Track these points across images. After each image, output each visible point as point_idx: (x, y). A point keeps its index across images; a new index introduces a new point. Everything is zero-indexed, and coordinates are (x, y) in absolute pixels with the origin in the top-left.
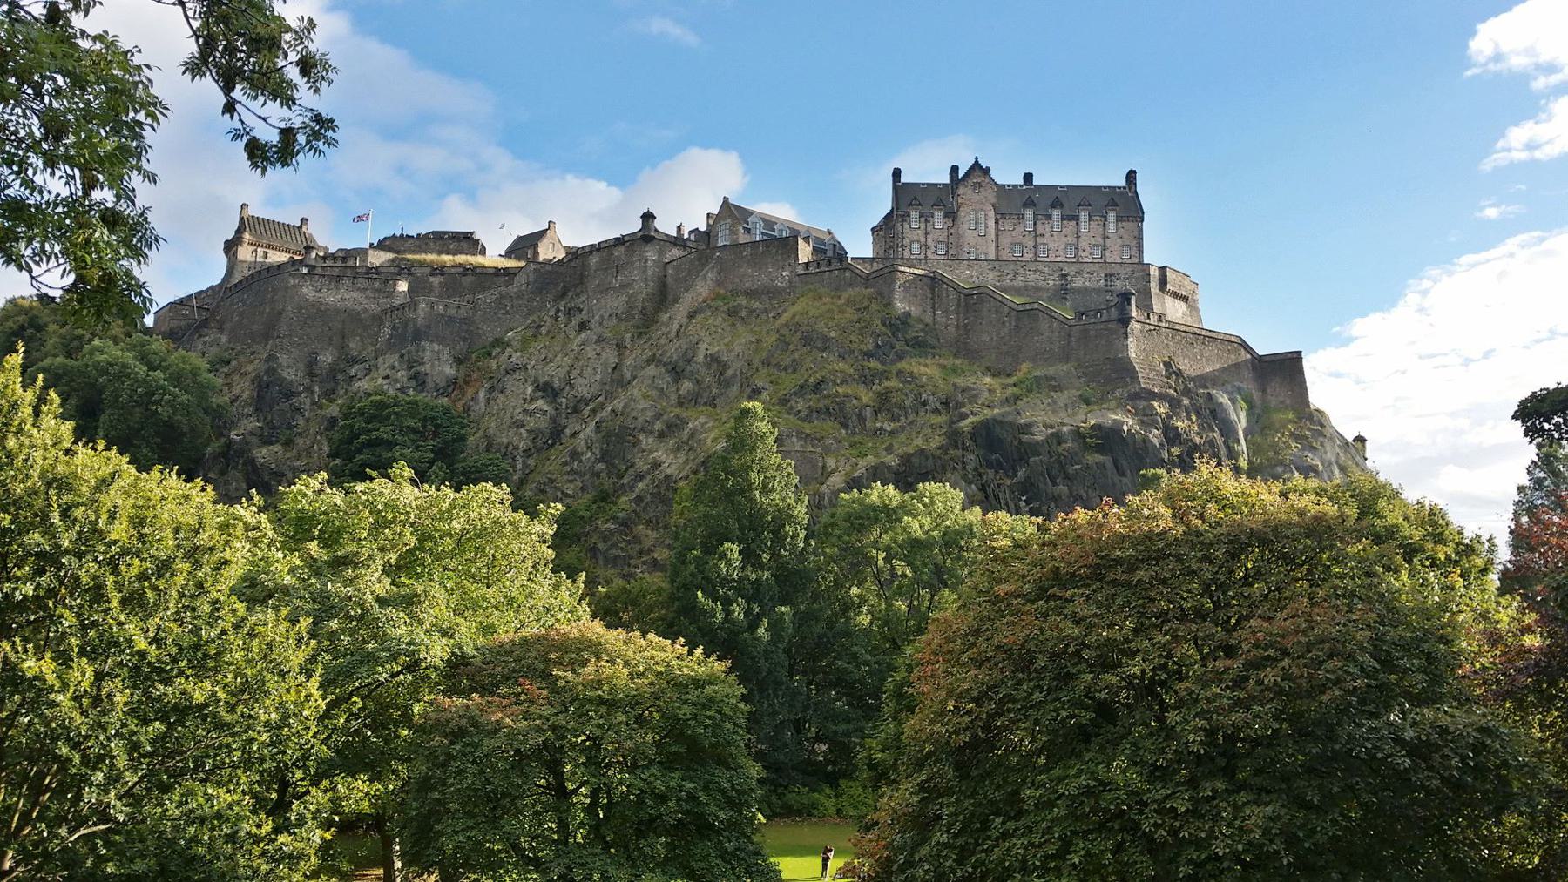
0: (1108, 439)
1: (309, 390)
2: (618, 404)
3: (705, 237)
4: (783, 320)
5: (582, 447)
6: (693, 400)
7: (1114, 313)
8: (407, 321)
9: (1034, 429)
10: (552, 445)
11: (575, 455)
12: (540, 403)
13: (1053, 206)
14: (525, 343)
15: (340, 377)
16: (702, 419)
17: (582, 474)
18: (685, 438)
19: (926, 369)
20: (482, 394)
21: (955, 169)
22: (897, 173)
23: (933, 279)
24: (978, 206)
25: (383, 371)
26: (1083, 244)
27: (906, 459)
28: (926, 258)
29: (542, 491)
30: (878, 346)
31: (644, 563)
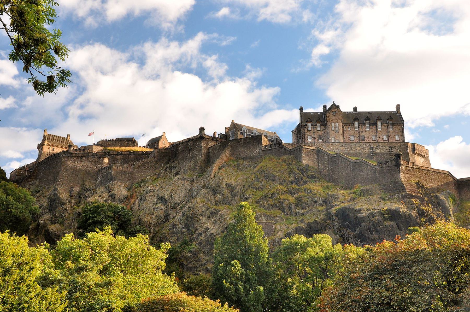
0: (394, 215)
1: (70, 202)
2: (191, 205)
3: (225, 137)
4: (256, 169)
6: (222, 202)
7: (394, 163)
9: (362, 211)
10: (165, 222)
11: (174, 226)
14: (154, 181)
15: (82, 196)
17: (177, 234)
18: (218, 218)
19: (317, 188)
21: (325, 106)
23: (318, 151)
24: (335, 121)
26: (379, 135)
27: (309, 225)
28: (314, 143)
30: (296, 178)
31: (203, 270)
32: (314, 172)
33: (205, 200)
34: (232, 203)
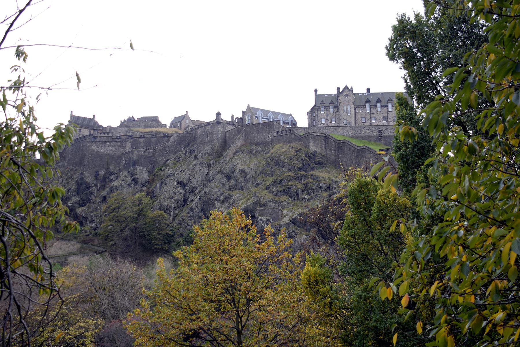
1: (96, 185)
2: (207, 190)
3: (241, 120)
4: (268, 155)
5: (194, 207)
8: (130, 158)
10: (184, 205)
11: (192, 209)
12: (179, 188)
13: (377, 102)
14: (174, 164)
15: (107, 180)
16: (238, 195)
17: (194, 217)
19: (322, 174)
20: (158, 185)
21: (338, 89)
22: (316, 91)
23: (325, 137)
24: (347, 103)
25: (122, 177)
26: (390, 116)
29: (180, 224)
30: (303, 165)
32: (321, 158)
33: (221, 185)
34: (245, 188)
